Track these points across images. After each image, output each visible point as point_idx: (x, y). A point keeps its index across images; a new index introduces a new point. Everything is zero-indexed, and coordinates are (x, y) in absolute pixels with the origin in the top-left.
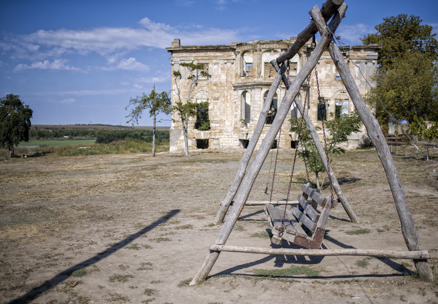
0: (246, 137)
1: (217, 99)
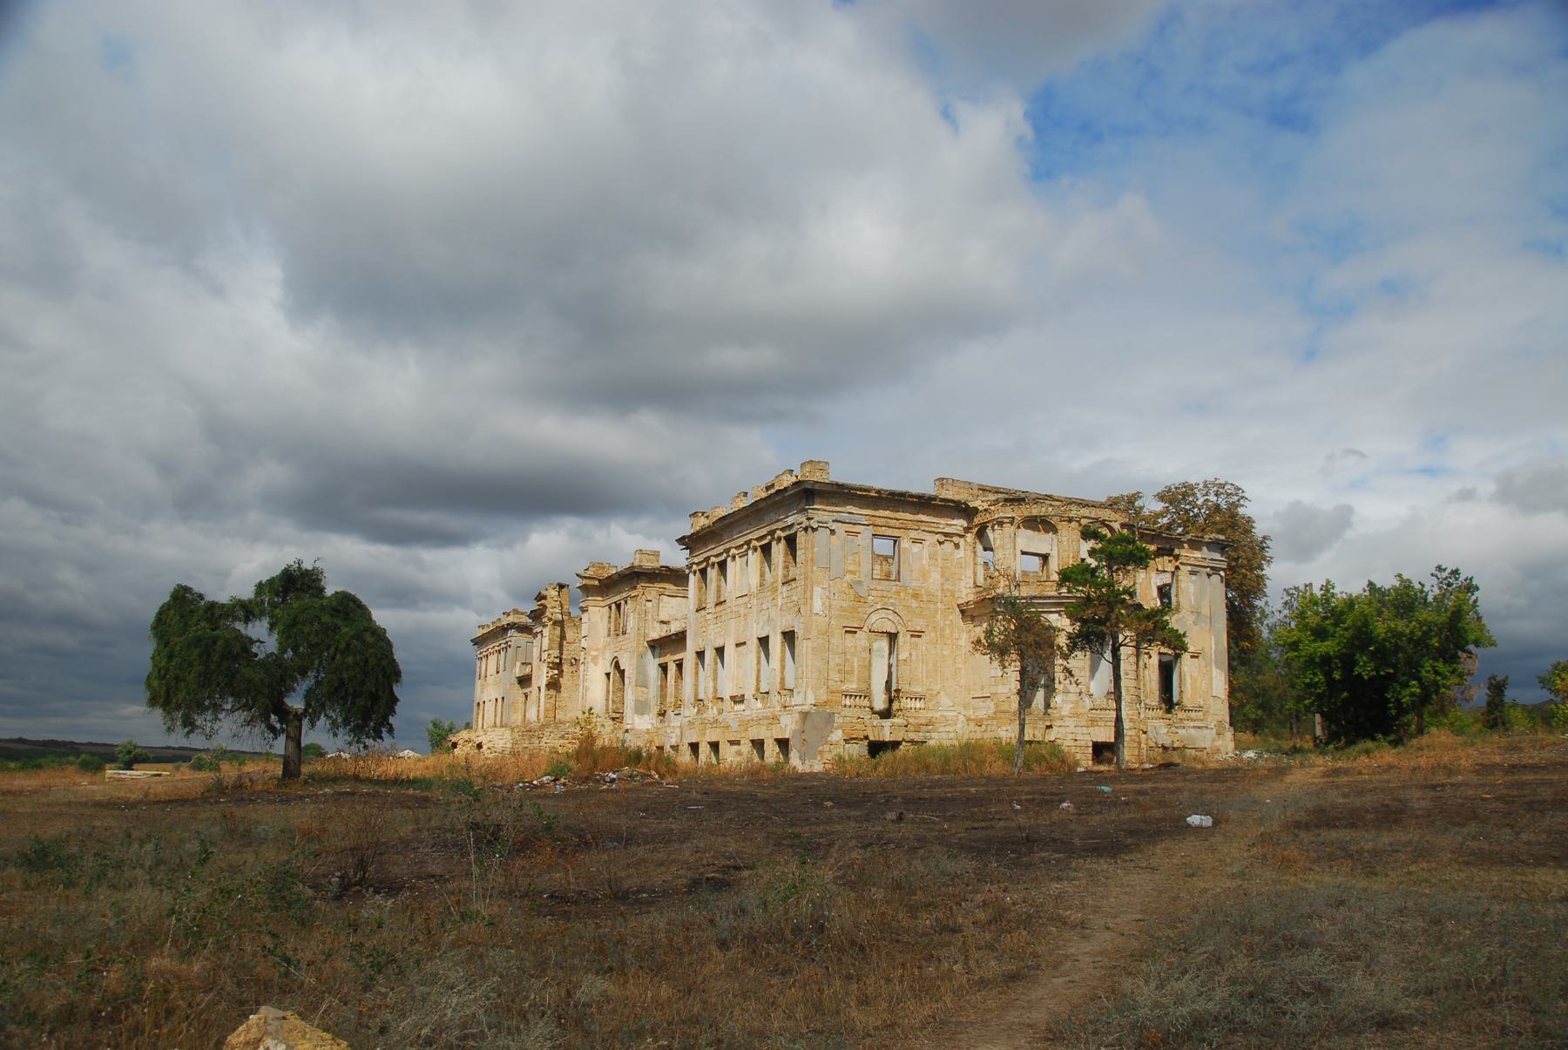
1: (917, 634)
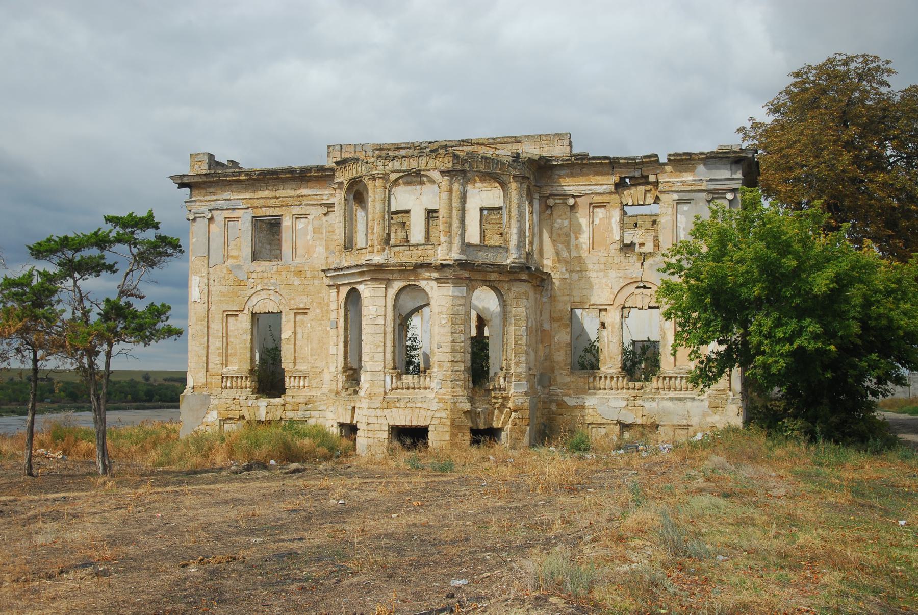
0: (353, 417)
1: (304, 312)
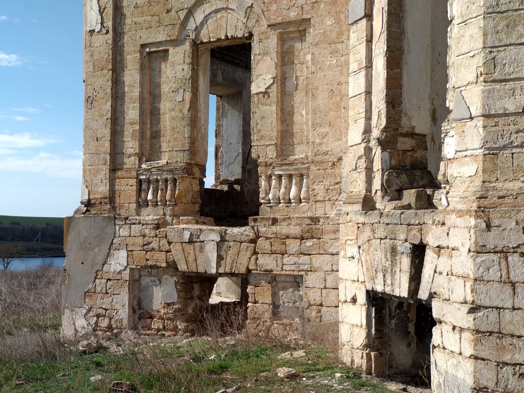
0: (416, 278)
